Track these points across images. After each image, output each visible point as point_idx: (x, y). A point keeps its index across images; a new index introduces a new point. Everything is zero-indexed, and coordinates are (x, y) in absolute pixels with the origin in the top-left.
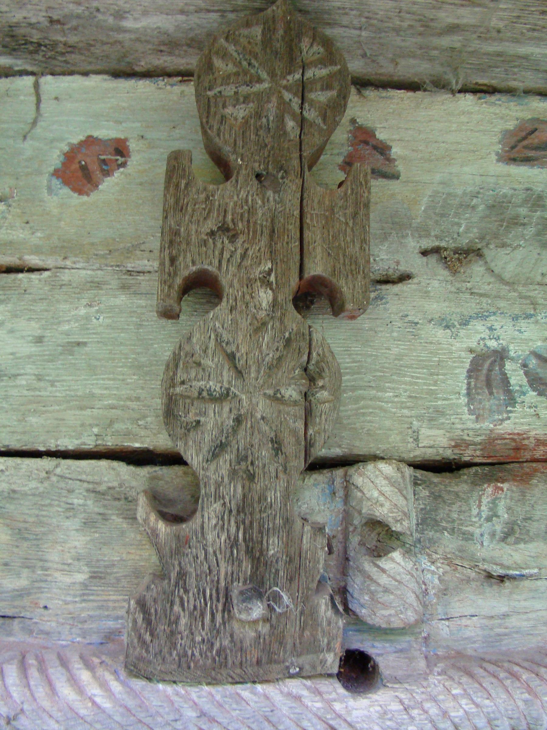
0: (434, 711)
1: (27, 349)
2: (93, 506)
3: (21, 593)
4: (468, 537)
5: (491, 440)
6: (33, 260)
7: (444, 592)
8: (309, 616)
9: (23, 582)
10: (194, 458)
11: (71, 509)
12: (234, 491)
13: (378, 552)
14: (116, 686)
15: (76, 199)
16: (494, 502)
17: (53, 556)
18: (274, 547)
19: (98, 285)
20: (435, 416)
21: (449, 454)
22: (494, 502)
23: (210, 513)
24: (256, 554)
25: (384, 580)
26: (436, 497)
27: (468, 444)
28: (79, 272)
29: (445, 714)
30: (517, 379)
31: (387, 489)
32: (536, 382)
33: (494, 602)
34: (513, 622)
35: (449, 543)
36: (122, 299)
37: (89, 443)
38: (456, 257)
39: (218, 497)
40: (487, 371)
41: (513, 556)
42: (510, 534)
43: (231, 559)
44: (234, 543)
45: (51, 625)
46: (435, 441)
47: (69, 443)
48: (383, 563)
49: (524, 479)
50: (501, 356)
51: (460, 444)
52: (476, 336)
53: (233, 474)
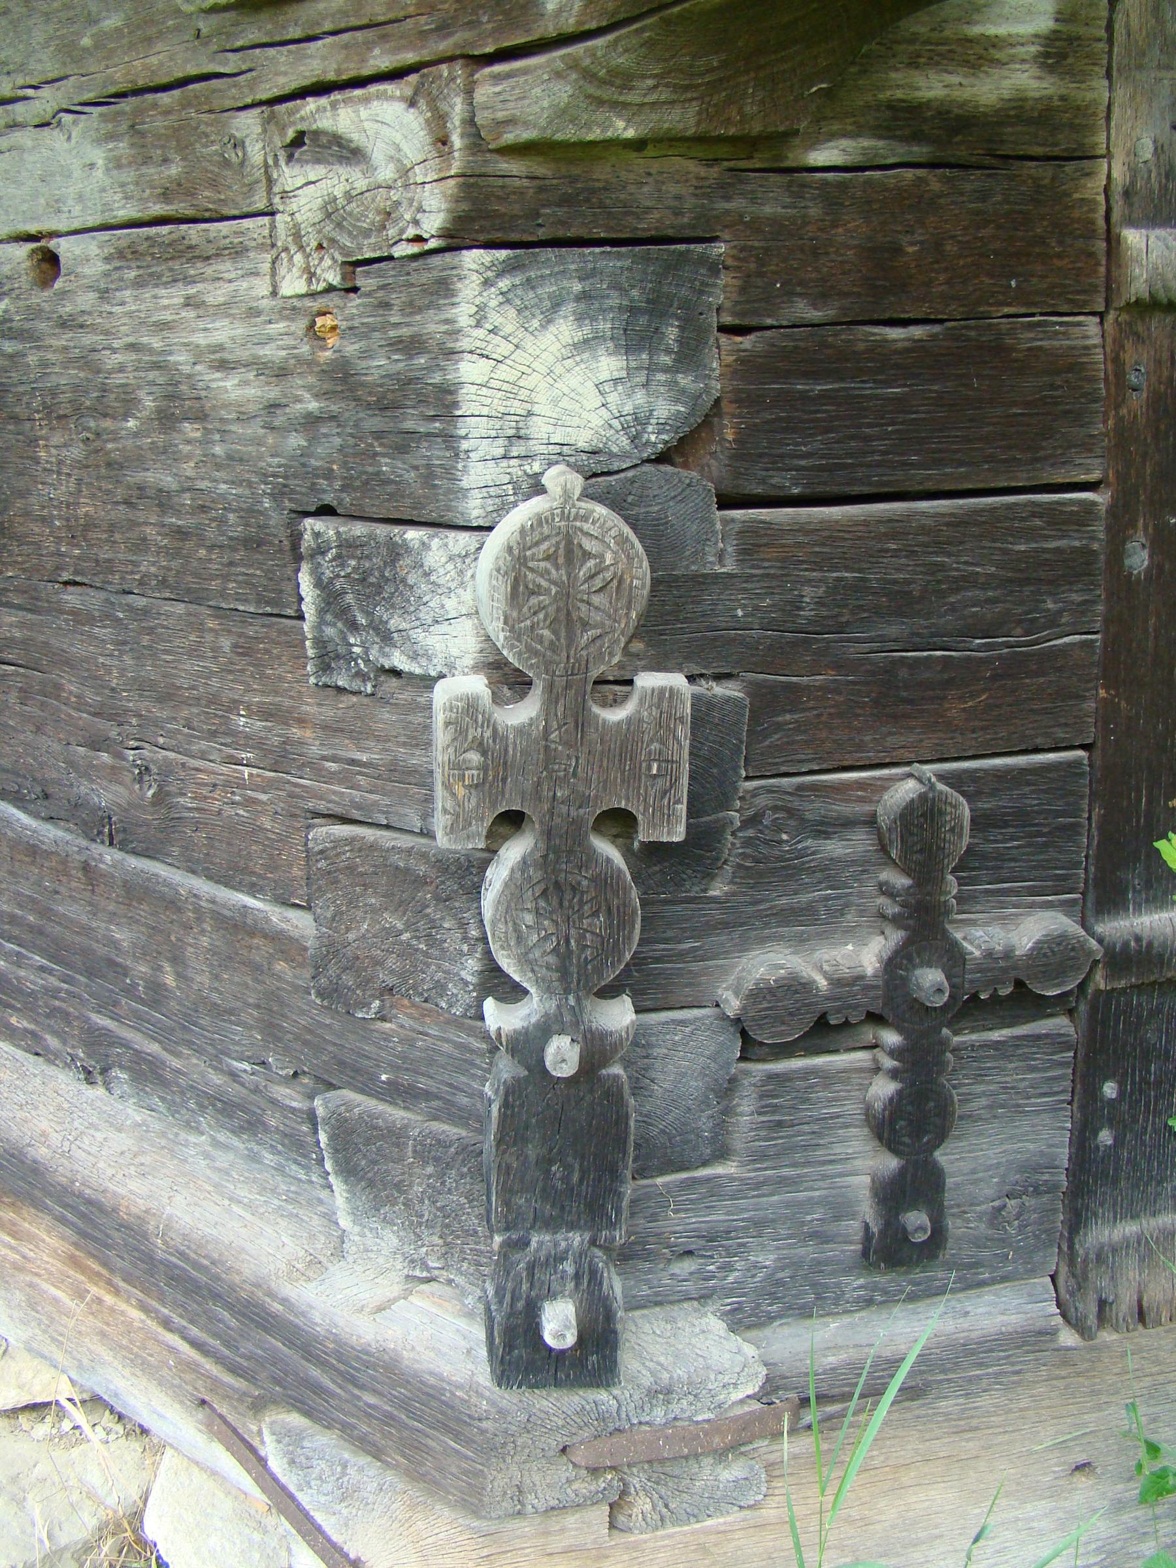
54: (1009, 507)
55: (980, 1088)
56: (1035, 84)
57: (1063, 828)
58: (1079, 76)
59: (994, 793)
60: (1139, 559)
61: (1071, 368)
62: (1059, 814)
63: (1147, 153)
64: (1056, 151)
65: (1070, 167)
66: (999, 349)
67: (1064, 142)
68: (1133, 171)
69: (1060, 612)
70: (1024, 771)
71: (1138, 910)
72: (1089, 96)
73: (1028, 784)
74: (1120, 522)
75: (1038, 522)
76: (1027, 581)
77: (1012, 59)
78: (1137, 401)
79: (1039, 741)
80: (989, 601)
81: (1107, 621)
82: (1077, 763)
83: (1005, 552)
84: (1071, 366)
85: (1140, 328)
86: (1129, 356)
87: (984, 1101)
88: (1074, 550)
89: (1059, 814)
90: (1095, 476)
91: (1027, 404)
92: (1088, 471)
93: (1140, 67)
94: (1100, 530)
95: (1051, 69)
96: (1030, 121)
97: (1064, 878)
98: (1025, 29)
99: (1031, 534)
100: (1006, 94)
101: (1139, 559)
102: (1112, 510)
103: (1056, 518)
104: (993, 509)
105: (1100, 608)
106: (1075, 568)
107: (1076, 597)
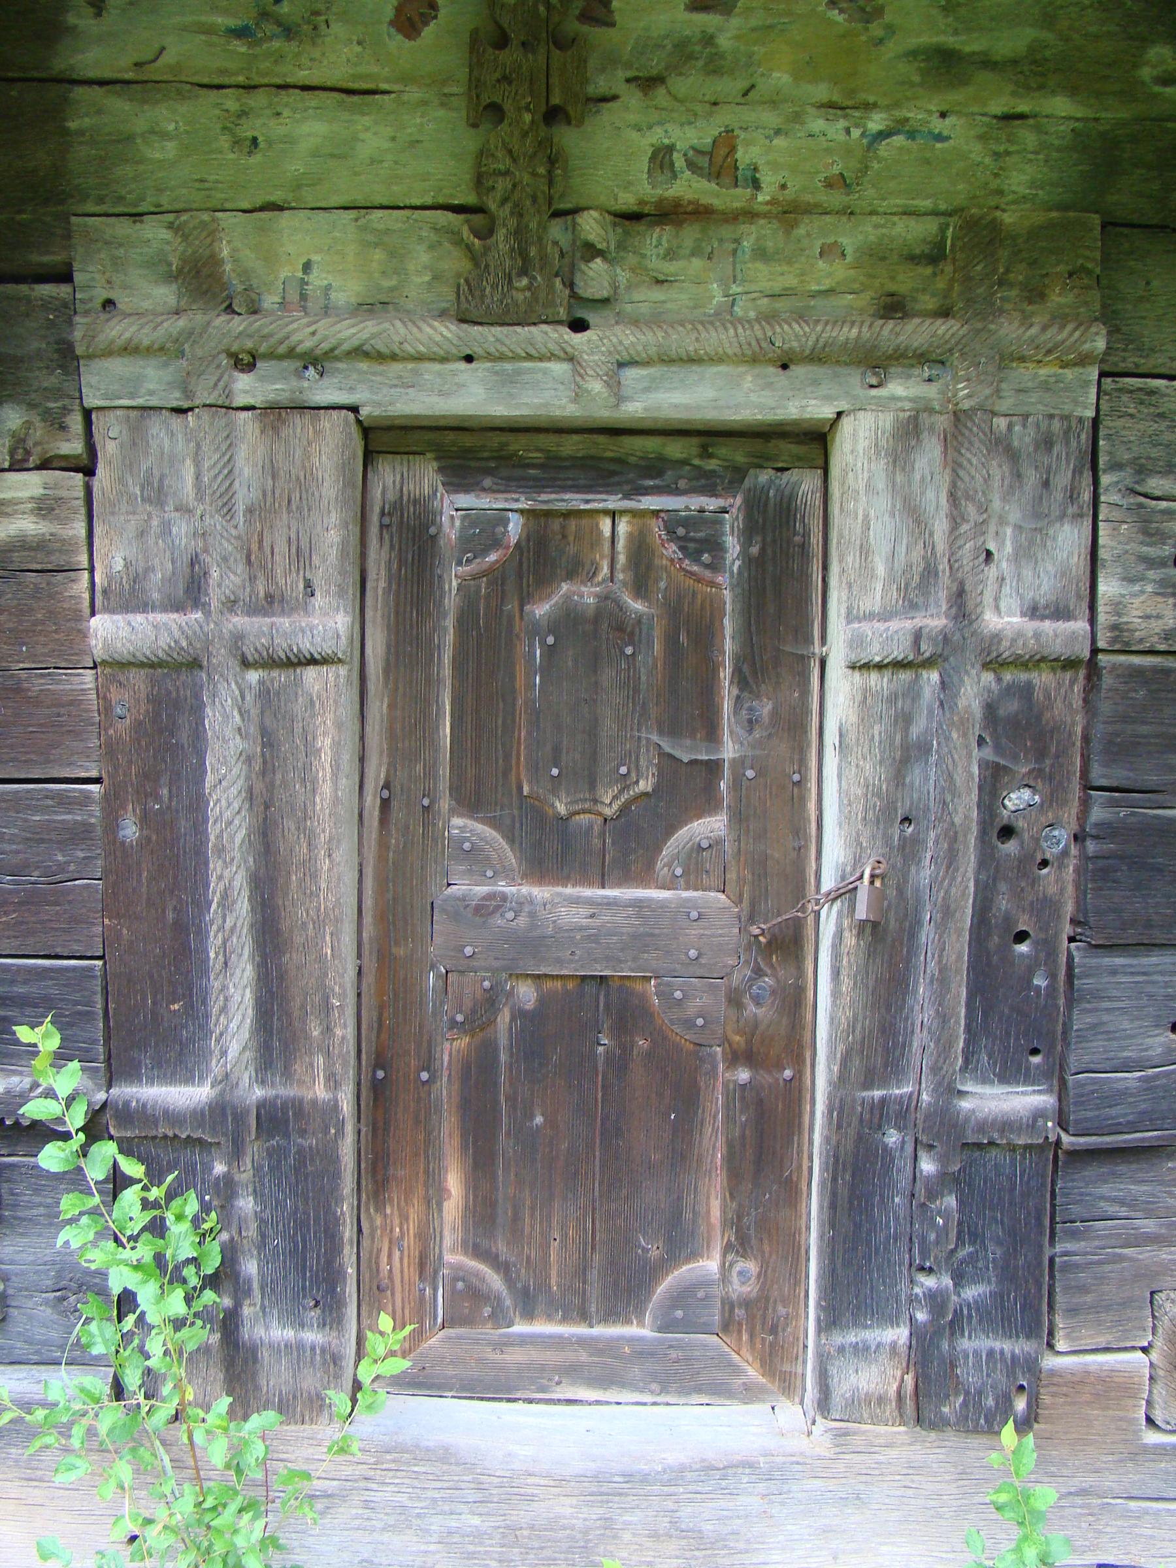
0: (615, 340)
1: (386, 145)
2: (434, 237)
3: (392, 289)
4: (644, 256)
5: (661, 201)
6: (384, 86)
7: (629, 288)
8: (551, 287)
9: (394, 283)
10: (493, 206)
11: (421, 238)
12: (512, 223)
13: (589, 259)
14: (453, 328)
15: (408, 44)
16: (660, 237)
17: (411, 267)
18: (533, 252)
19: (424, 103)
20: (627, 186)
21: (635, 208)
22: (660, 237)
23: (501, 233)
24: (523, 254)
25: (591, 273)
26: (627, 233)
27: (646, 203)
28: (414, 94)
29: (621, 342)
30: (679, 162)
31: (595, 225)
32: (691, 165)
33: (657, 294)
34: (669, 306)
35: (632, 259)
36: (441, 113)
37: (429, 201)
38: (648, 83)
39: (504, 225)
40: (662, 158)
41: (670, 268)
42: (670, 255)
43: (512, 258)
44: (512, 250)
45: (411, 306)
46: (627, 201)
47: (417, 202)
48: (592, 265)
49: (678, 224)
50: (670, 149)
51: (641, 202)
52: (657, 136)
53: (512, 214)
54: (28, 791)
55: (38, 1199)
56: (32, 526)
57: (79, 1013)
58: (64, 521)
59: (26, 982)
60: (130, 830)
61: (71, 703)
62: (77, 1003)
63: (119, 565)
64: (50, 567)
65: (60, 577)
66: (18, 690)
67: (57, 560)
68: (110, 578)
69: (68, 863)
70: (46, 970)
71: (151, 1081)
72: (71, 533)
73: (52, 979)
74: (112, 806)
75: (50, 802)
76: (42, 841)
77: (16, 512)
78: (122, 728)
79: (59, 950)
80: (18, 852)
81: (106, 871)
82: (91, 969)
83: (26, 820)
84: (75, 702)
85: (122, 678)
86: (114, 695)
87: (42, 1210)
88: (76, 822)
89: (77, 1003)
90: (94, 774)
91: (41, 725)
92: (87, 770)
93: (113, 513)
94: (96, 809)
95: (44, 517)
96: (31, 549)
97: (88, 1050)
98: (26, 494)
99: (45, 810)
100: (12, 533)
101: (130, 830)
102: (106, 797)
103: (64, 801)
104: (17, 792)
105: (99, 862)
106: (79, 834)
107: (81, 854)
